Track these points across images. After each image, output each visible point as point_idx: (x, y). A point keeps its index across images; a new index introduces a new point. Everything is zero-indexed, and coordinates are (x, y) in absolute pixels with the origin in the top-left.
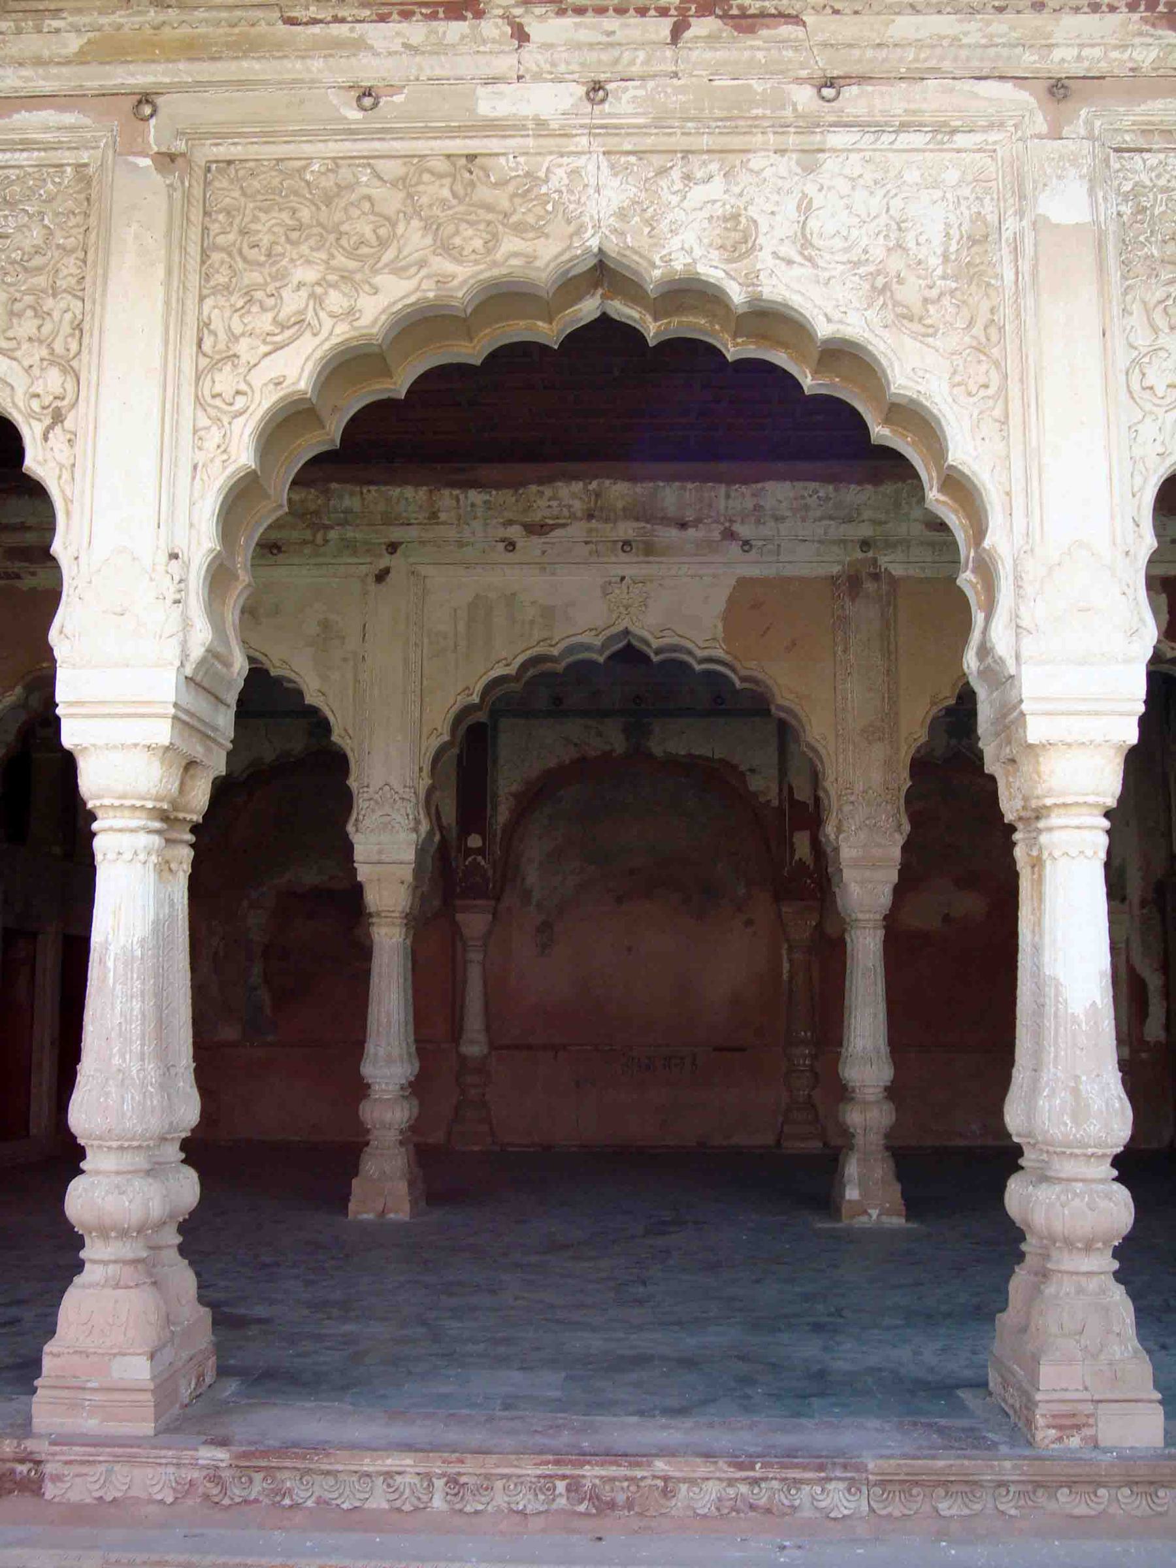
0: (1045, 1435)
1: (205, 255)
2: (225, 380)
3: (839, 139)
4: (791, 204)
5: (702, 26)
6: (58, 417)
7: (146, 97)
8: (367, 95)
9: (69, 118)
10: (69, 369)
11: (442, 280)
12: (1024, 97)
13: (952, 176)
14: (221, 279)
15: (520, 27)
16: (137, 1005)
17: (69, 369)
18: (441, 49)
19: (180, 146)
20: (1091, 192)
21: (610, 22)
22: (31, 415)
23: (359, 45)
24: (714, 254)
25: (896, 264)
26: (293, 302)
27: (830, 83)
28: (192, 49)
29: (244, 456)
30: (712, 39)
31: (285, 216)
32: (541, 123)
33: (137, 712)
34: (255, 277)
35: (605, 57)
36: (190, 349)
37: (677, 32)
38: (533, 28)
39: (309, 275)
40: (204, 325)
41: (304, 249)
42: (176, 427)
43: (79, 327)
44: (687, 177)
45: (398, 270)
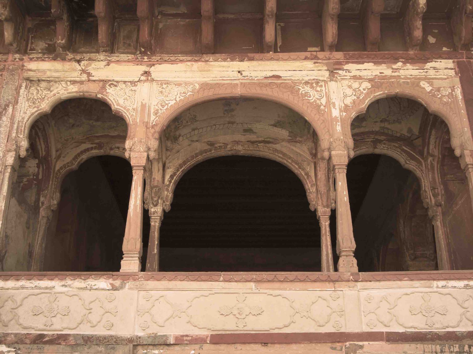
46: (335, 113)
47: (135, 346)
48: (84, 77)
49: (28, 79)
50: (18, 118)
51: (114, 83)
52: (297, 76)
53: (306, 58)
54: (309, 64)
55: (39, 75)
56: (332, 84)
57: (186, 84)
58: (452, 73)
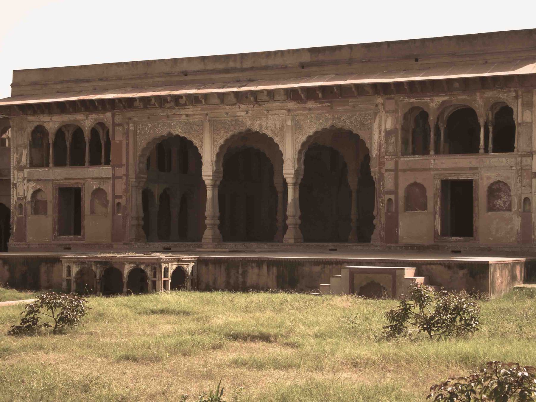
0: (284, 242)
1: (213, 130)
2: (216, 143)
3: (270, 116)
4: (266, 123)
5: (256, 105)
6: (201, 147)
7: (207, 114)
8: (227, 114)
9: (200, 116)
10: (202, 142)
11: (235, 132)
12: (286, 111)
13: (280, 119)
14: (215, 132)
15: (239, 106)
16: (210, 204)
17: (202, 142)
18: (233, 109)
19: (210, 119)
20: (292, 122)
21: (248, 105)
22: (199, 147)
23: (225, 109)
24: (259, 129)
25: (275, 129)
26: (222, 134)
27: (268, 111)
28: (211, 109)
29: (218, 150)
30: (257, 107)
31: (220, 126)
32: (242, 116)
33: (209, 176)
34: (218, 132)
35: (248, 109)
36: (212, 140)
37: (254, 106)
38: (241, 106)
39: (222, 132)
40: (214, 137)
41: (222, 129)
42: (211, 147)
43: (203, 137)
44: (256, 121)
45: (231, 131)
46: (87, 129)
47: (53, 181)
48: (39, 120)
49: (29, 121)
50: (28, 131)
51: (44, 122)
52: (81, 118)
53: (82, 114)
54: (82, 115)
55: (30, 120)
56: (87, 120)
57: (59, 121)
58: (110, 116)
